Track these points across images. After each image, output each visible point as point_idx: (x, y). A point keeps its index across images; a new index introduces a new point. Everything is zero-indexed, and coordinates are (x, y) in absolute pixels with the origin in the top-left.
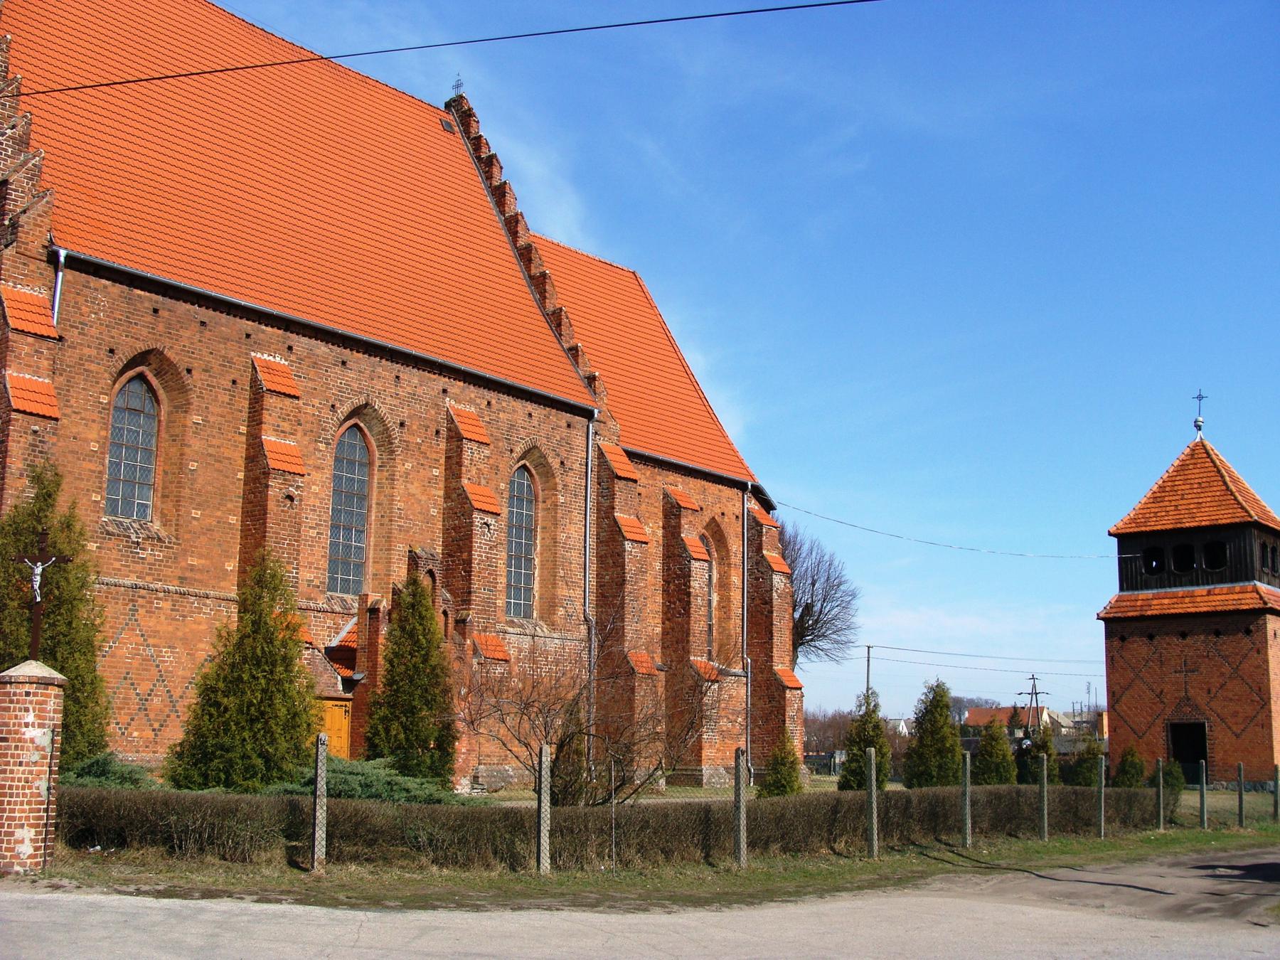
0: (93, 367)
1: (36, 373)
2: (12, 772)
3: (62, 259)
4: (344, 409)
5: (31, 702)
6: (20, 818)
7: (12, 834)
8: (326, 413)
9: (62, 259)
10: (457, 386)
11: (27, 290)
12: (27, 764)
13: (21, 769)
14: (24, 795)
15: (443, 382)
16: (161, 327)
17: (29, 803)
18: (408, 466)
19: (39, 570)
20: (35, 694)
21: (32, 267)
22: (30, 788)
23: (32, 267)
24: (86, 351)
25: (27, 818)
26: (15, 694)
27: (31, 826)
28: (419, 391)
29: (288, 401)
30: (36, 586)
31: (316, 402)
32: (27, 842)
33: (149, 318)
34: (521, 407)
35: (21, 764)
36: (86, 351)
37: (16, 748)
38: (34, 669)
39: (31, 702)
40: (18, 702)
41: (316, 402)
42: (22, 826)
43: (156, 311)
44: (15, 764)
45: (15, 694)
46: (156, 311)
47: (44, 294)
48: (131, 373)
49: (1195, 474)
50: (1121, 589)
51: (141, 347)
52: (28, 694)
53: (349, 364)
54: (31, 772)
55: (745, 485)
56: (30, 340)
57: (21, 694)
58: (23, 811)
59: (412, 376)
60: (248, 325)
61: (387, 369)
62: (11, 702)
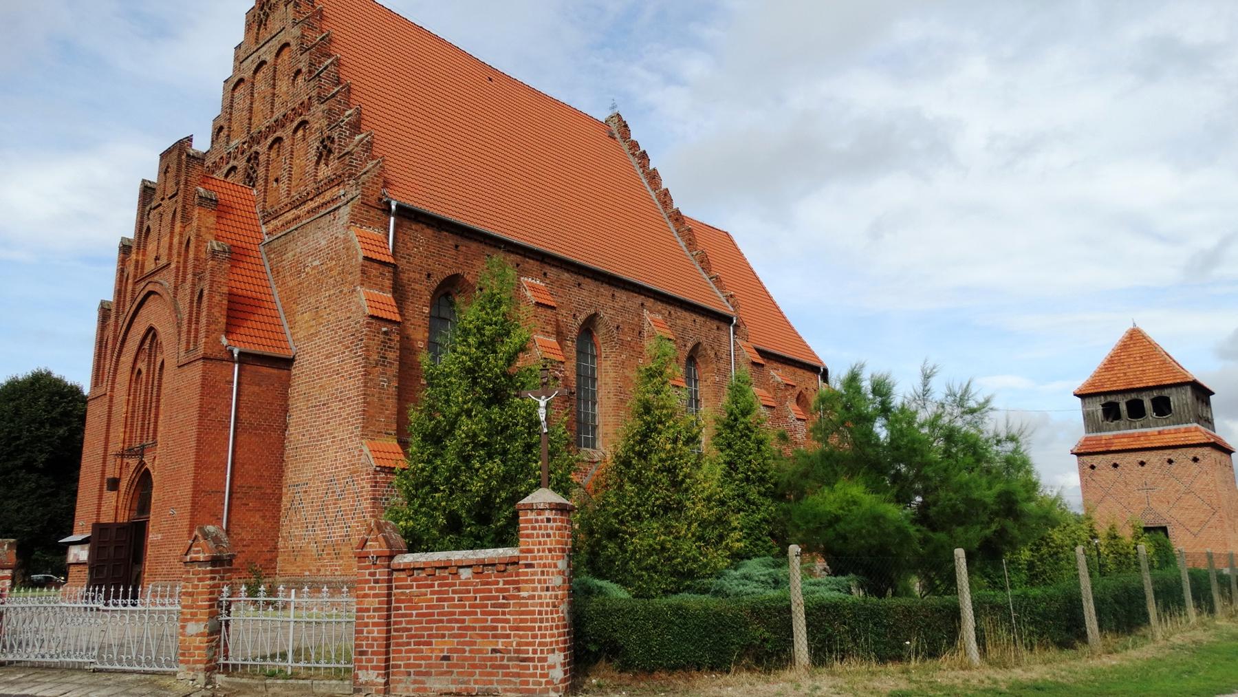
0: (417, 287)
1: (381, 290)
2: (540, 597)
3: (393, 207)
4: (582, 318)
5: (552, 528)
6: (551, 643)
7: (545, 660)
8: (570, 320)
9: (393, 207)
10: (649, 302)
11: (370, 231)
12: (553, 589)
13: (548, 593)
14: (553, 619)
15: (640, 299)
16: (461, 259)
17: (557, 627)
18: (624, 356)
19: (542, 403)
20: (555, 520)
21: (372, 213)
22: (557, 612)
23: (372, 213)
24: (412, 275)
25: (557, 642)
26: (537, 521)
27: (560, 650)
28: (627, 305)
29: (549, 311)
30: (543, 418)
31: (564, 312)
32: (558, 666)
33: (454, 252)
34: (688, 317)
35: (548, 589)
36: (412, 275)
37: (543, 573)
38: (544, 496)
39: (552, 528)
40: (540, 528)
41: (564, 312)
42: (553, 651)
43: (457, 246)
44: (542, 590)
45: (537, 521)
46: (457, 246)
47: (381, 235)
48: (442, 292)
49: (1136, 351)
50: (1087, 431)
51: (449, 272)
52: (548, 520)
53: (583, 286)
54: (556, 597)
55: (819, 368)
56: (376, 265)
57: (542, 521)
58: (552, 636)
59: (622, 296)
60: (518, 258)
61: (605, 290)
62: (534, 528)
